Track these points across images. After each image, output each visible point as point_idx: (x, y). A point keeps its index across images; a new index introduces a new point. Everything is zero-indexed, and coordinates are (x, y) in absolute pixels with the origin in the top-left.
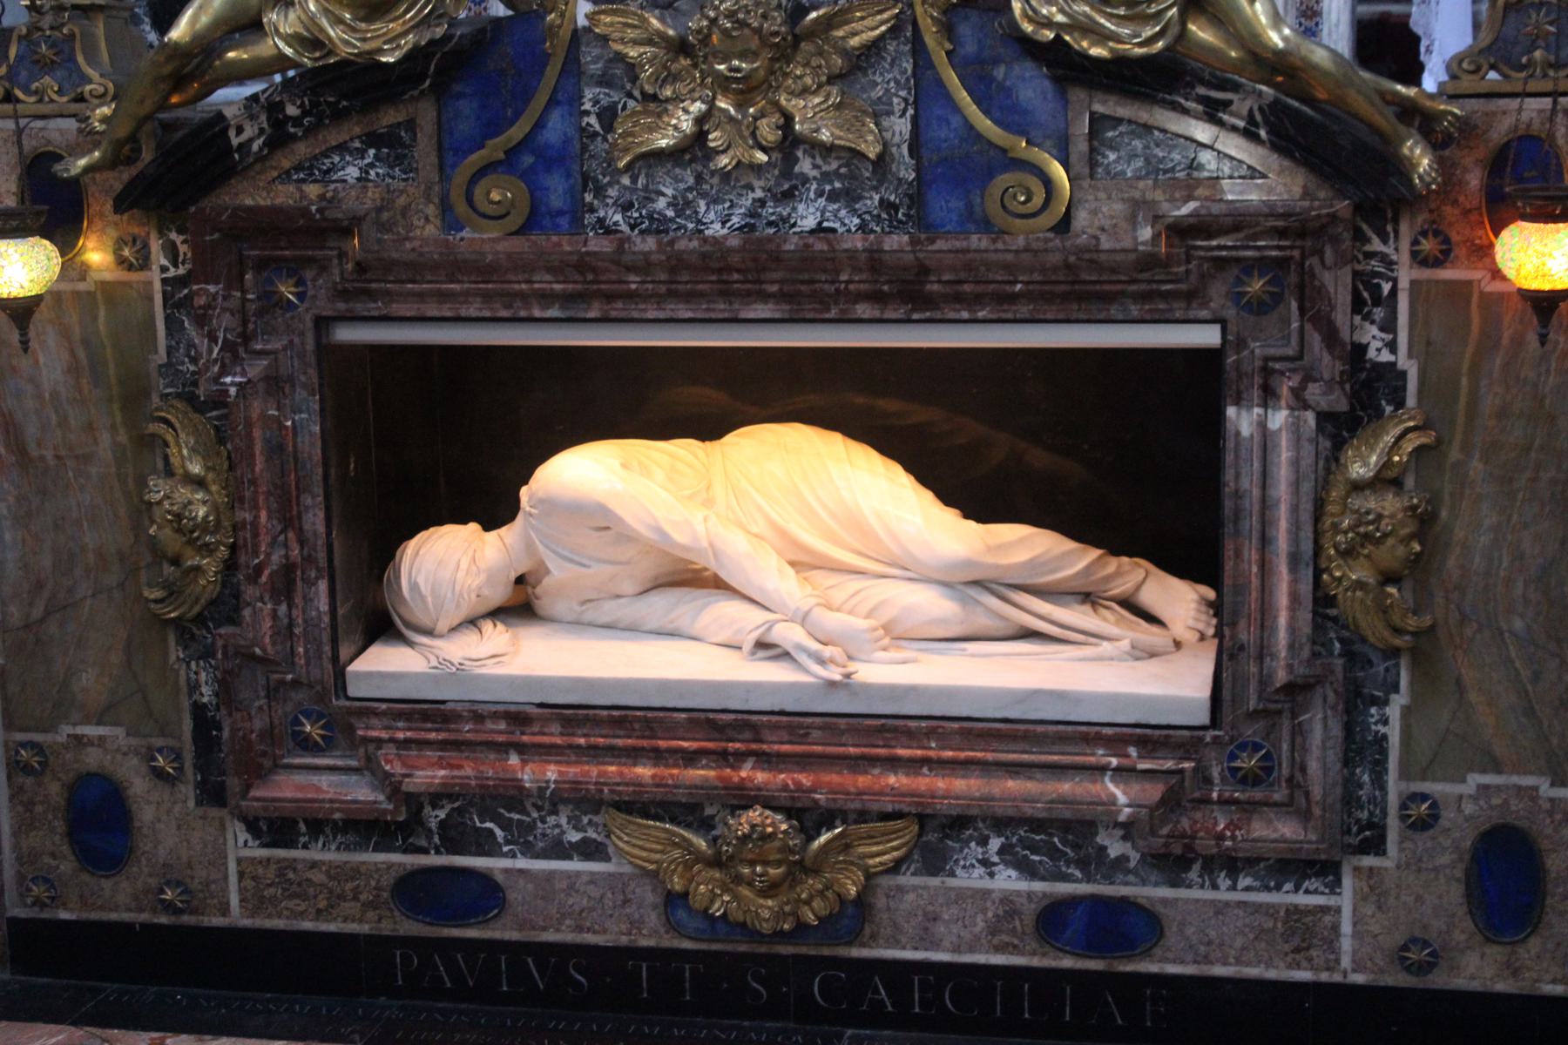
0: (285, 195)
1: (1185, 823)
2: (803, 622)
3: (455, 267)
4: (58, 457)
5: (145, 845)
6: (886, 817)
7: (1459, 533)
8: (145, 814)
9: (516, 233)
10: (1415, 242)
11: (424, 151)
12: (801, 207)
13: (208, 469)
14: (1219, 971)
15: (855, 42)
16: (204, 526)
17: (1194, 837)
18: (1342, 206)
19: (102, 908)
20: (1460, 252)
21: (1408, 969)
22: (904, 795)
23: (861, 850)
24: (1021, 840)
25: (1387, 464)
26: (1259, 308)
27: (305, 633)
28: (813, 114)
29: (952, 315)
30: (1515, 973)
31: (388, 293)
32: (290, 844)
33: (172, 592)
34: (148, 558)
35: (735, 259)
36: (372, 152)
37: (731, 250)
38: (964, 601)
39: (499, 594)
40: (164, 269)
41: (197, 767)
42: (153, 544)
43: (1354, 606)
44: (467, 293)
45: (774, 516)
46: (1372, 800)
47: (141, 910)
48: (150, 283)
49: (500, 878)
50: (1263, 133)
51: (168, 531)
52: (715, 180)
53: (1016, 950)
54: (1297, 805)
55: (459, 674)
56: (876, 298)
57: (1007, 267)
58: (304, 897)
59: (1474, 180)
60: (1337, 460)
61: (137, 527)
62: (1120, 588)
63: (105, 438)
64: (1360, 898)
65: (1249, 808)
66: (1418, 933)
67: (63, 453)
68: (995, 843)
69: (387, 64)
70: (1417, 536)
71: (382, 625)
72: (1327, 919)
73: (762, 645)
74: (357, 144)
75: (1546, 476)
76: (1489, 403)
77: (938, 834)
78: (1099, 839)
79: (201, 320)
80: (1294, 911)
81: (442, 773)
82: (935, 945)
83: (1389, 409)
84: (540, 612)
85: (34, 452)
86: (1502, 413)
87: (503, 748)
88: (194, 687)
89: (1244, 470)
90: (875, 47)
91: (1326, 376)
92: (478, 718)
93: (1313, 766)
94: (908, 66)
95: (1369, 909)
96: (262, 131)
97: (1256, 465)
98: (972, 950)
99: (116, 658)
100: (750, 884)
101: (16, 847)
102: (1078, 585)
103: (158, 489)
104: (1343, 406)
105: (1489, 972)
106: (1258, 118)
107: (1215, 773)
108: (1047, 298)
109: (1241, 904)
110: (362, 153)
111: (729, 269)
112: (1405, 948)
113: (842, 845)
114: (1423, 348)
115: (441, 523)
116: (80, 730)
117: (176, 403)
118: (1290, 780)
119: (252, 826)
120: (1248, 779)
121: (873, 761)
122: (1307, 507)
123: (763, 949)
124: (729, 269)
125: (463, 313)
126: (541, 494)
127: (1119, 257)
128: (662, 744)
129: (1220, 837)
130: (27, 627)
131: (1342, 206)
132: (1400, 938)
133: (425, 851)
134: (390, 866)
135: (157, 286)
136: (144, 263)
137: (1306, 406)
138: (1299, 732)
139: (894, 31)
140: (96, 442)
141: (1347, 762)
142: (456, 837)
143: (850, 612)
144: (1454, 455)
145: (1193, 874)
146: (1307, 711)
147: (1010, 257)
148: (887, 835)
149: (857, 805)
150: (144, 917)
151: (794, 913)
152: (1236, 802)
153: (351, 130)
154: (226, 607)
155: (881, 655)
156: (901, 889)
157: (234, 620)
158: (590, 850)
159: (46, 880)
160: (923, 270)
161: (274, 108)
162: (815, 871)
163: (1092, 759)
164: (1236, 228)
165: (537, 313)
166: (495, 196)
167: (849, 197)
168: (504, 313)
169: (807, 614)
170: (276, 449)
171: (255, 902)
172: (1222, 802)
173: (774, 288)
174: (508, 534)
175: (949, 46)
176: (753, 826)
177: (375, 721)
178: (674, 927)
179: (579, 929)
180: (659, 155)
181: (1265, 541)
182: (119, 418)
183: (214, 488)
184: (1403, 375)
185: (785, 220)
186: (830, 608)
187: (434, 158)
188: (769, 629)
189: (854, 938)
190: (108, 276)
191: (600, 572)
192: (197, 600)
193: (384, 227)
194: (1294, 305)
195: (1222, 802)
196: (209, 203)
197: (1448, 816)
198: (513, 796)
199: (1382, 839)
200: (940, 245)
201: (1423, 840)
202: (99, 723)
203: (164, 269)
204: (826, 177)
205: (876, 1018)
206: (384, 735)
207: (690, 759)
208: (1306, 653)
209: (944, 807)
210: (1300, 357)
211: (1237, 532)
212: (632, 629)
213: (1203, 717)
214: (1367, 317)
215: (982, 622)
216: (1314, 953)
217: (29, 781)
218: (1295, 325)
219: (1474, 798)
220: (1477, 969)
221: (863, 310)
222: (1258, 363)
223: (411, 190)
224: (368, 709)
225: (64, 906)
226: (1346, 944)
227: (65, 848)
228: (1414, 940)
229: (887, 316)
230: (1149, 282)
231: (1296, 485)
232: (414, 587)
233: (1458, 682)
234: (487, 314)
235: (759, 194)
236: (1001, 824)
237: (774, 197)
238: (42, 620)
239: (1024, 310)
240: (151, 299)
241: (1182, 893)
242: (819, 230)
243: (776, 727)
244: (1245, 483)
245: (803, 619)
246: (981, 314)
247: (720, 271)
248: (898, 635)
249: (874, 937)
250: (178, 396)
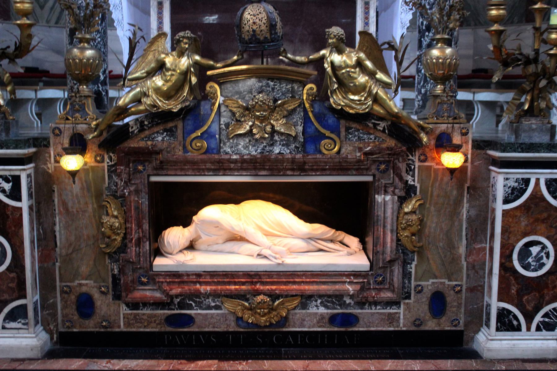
0: (142, 144)
1: (365, 294)
2: (269, 249)
3: (186, 162)
4: (77, 211)
5: (98, 311)
6: (293, 296)
7: (428, 223)
8: (98, 303)
9: (201, 154)
10: (419, 157)
11: (180, 132)
12: (275, 148)
13: (119, 214)
14: (372, 329)
15: (290, 108)
16: (118, 229)
17: (368, 297)
18: (404, 148)
19: (86, 328)
20: (429, 159)
21: (415, 326)
22: (298, 290)
23: (287, 304)
24: (325, 300)
25: (413, 208)
26: (385, 171)
27: (143, 255)
28: (279, 125)
29: (311, 174)
30: (439, 325)
31: (168, 169)
32: (138, 309)
33: (108, 246)
34: (101, 236)
35: (259, 160)
36: (165, 133)
37: (258, 158)
38: (308, 243)
39: (187, 244)
40: (108, 163)
41: (113, 290)
42: (103, 233)
43: (404, 241)
44: (188, 169)
46: (408, 287)
47: (96, 328)
48: (104, 167)
49: (193, 316)
50: (387, 131)
51: (108, 230)
52: (254, 141)
53: (324, 327)
54: (391, 289)
55: (183, 265)
56: (293, 170)
57: (325, 162)
58: (141, 323)
59: (433, 142)
60: (401, 207)
61: (98, 229)
62: (339, 239)
63: (90, 206)
64: (405, 310)
65: (380, 290)
66: (418, 317)
67: (79, 210)
68: (319, 301)
69: (174, 112)
70: (420, 225)
71: (158, 252)
72: (397, 315)
73: (258, 255)
74: (161, 131)
75: (447, 210)
76: (435, 194)
77: (306, 299)
78: (344, 299)
79: (119, 175)
80: (390, 314)
81: (180, 289)
82: (304, 327)
83: (413, 195)
84: (196, 248)
85: (70, 210)
86: (438, 196)
87: (195, 283)
88: (113, 270)
89: (379, 210)
90: (294, 110)
91: (400, 187)
92: (188, 275)
93: (395, 279)
94: (302, 114)
95: (407, 312)
96: (138, 128)
97: (383, 209)
98: (313, 327)
99: (91, 263)
100: (259, 314)
101: (62, 313)
102: (331, 238)
103: (105, 219)
104: (404, 195)
105: (434, 325)
106: (386, 127)
107: (371, 282)
108: (334, 170)
109: (378, 313)
110: (163, 134)
111: (256, 163)
112: (415, 321)
113: (282, 303)
114: (421, 181)
115: (173, 226)
116: (81, 282)
117: (110, 197)
118: (389, 283)
119: (127, 305)
120: (381, 283)
121: (289, 282)
122: (395, 218)
123: (261, 330)
124: (256, 163)
125: (187, 173)
126: (202, 219)
127: (352, 160)
128: (236, 280)
129: (374, 297)
130: (67, 255)
131: (404, 148)
132: (414, 319)
133: (174, 310)
134: (164, 314)
135: (106, 167)
136: (103, 161)
137: (395, 195)
138: (392, 271)
139: (299, 106)
140: (88, 207)
141: (403, 278)
142: (182, 306)
143: (279, 246)
144: (428, 206)
145: (366, 306)
146: (393, 266)
147: (326, 160)
148: (293, 300)
149: (286, 293)
150: (97, 330)
151: (270, 321)
152: (377, 289)
153: (160, 128)
154: (123, 248)
156: (296, 314)
157: (124, 252)
158: (217, 307)
159: (70, 321)
160: (305, 163)
161: (142, 123)
162: (275, 310)
163: (343, 280)
164: (379, 153)
165: (206, 173)
166: (198, 144)
167: (287, 145)
168: (198, 174)
170: (137, 208)
171: (127, 324)
172: (373, 289)
173: (268, 167)
175: (312, 110)
176: (262, 300)
177: (161, 277)
178: (238, 326)
179: (214, 327)
180: (240, 135)
181: (384, 227)
182: (94, 201)
183: (120, 219)
184: (416, 187)
185: (271, 151)
186: (275, 245)
187: (182, 135)
189: (284, 326)
190: (92, 164)
191: (214, 238)
192: (115, 247)
193: (168, 152)
194: (392, 171)
195: (373, 289)
196: (122, 146)
197: (425, 290)
198: (197, 295)
199: (410, 295)
200: (310, 157)
201: (419, 296)
202: (86, 280)
203: (108, 163)
204: (282, 140)
205: (289, 345)
206: (164, 280)
207: (243, 284)
208: (394, 253)
209: (308, 293)
210: (393, 183)
211: (377, 225)
212: (221, 252)
213: (368, 269)
214: (408, 174)
215: (312, 248)
216: (394, 323)
217: (66, 296)
218: (392, 176)
219: (431, 285)
220: (431, 325)
221: (289, 172)
222: (383, 185)
223: (175, 143)
224: (159, 274)
225: (75, 328)
226: (401, 321)
227: (76, 313)
228: (417, 319)
229: (295, 174)
230: (359, 165)
231: (393, 213)
232: (168, 243)
233: (428, 258)
234: (193, 174)
235: (265, 144)
236: (320, 296)
237: (269, 145)
238: (71, 254)
239: (328, 173)
240: (104, 170)
241: (364, 311)
242: (280, 153)
243: (264, 275)
244: (379, 213)
246: (318, 173)
247: (254, 163)
248: (292, 251)
249: (289, 326)
250: (111, 195)
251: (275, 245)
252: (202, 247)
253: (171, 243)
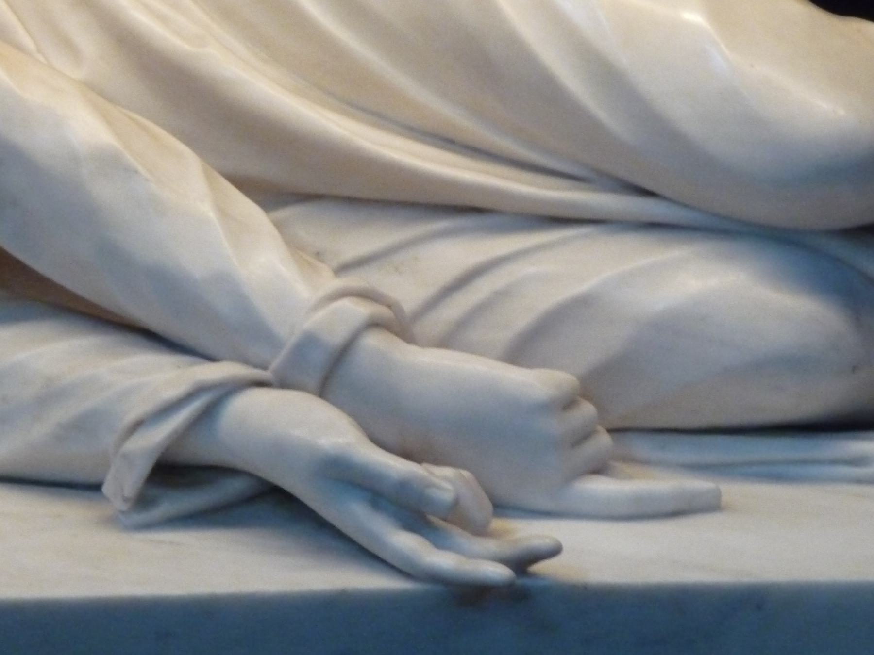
45: (141, 19)
73: (171, 473)
143: (446, 342)
155: (600, 487)
169: (342, 354)
186: (399, 325)
188: (209, 414)
245: (327, 371)
251: (399, 325)
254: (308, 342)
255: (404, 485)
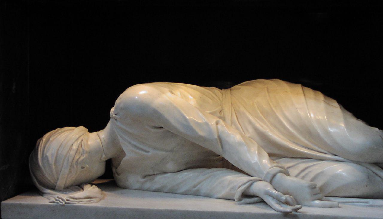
2: (271, 182)
45: (257, 125)
126: (121, 105)
155: (317, 202)
169: (274, 176)
174: (103, 134)
188: (251, 184)
212: (172, 192)
232: (45, 158)
252: (133, 180)
253: (51, 160)
254: (268, 173)
255: (277, 196)
